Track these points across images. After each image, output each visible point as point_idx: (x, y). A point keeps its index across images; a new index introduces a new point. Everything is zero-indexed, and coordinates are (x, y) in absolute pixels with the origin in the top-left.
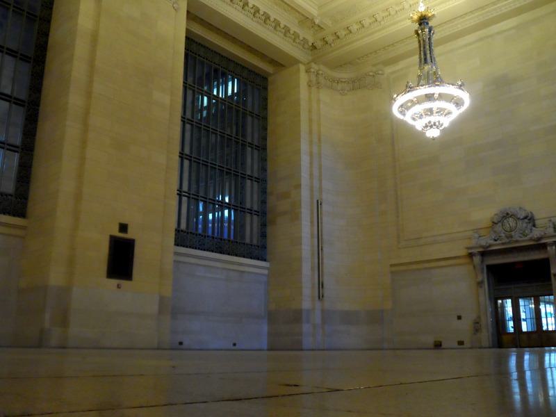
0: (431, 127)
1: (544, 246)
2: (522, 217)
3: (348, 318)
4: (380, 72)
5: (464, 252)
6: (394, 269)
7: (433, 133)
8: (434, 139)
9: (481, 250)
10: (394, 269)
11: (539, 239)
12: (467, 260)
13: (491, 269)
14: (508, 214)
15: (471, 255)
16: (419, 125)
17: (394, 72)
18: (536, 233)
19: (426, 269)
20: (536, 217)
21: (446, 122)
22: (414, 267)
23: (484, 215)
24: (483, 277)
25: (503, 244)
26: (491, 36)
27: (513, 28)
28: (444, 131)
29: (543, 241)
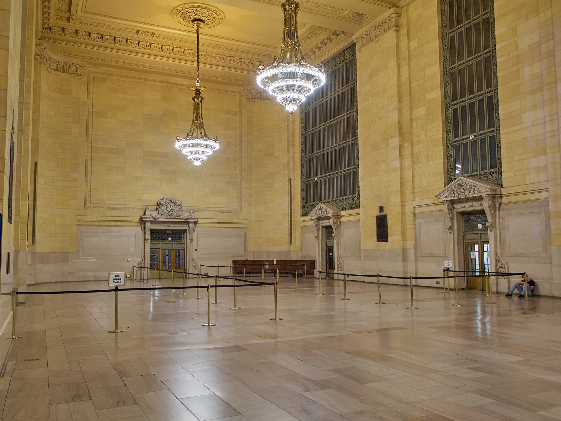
0: (197, 160)
1: (188, 223)
3: (44, 258)
4: (85, 68)
5: (137, 219)
6: (80, 223)
9: (152, 220)
10: (80, 223)
11: (187, 219)
12: (138, 224)
13: (153, 232)
15: (142, 221)
17: (93, 72)
18: (185, 215)
19: (106, 226)
20: (183, 205)
22: (97, 223)
23: (152, 198)
24: (148, 236)
25: (166, 218)
26: (170, 83)
27: (184, 85)
29: (188, 220)
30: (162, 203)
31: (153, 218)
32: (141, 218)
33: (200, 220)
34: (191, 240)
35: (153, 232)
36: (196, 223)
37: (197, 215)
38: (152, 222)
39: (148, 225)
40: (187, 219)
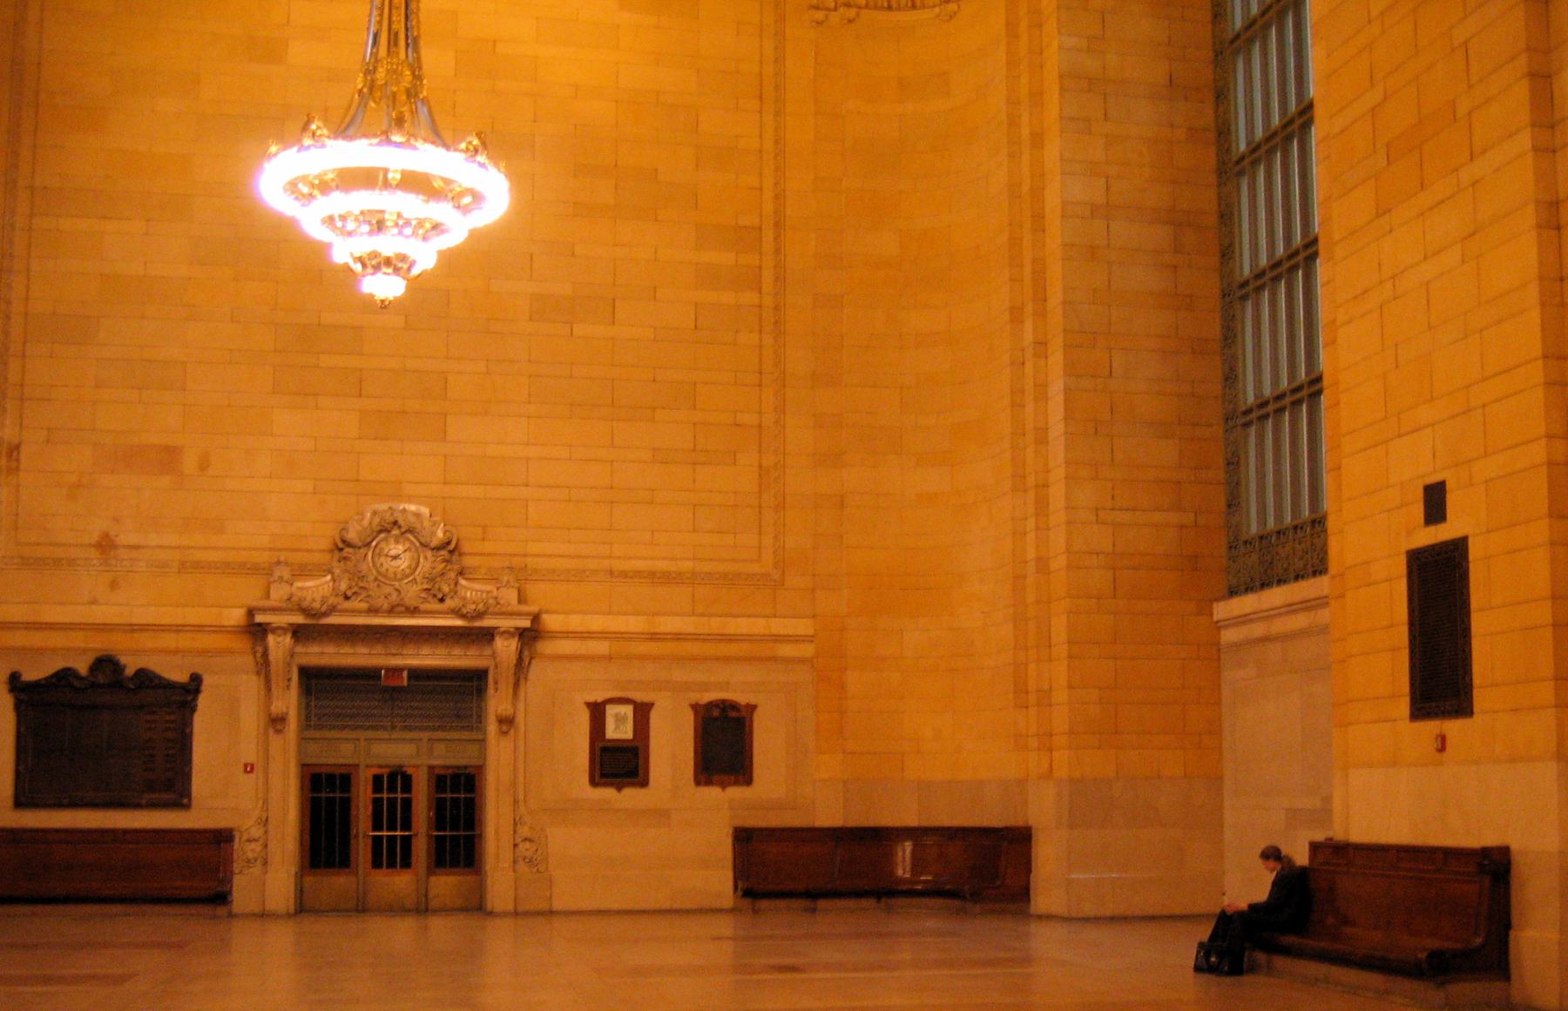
1: (488, 635)
2: (434, 543)
5: (236, 616)
7: (385, 287)
8: (384, 305)
9: (299, 619)
11: (480, 615)
12: (241, 644)
13: (314, 680)
14: (395, 523)
15: (256, 631)
16: (343, 252)
21: (425, 257)
24: (288, 701)
28: (417, 286)
29: (487, 622)
30: (352, 536)
31: (305, 611)
32: (251, 613)
33: (551, 622)
34: (507, 722)
35: (314, 680)
36: (530, 636)
37: (541, 595)
38: (299, 633)
39: (278, 645)
40: (480, 615)
